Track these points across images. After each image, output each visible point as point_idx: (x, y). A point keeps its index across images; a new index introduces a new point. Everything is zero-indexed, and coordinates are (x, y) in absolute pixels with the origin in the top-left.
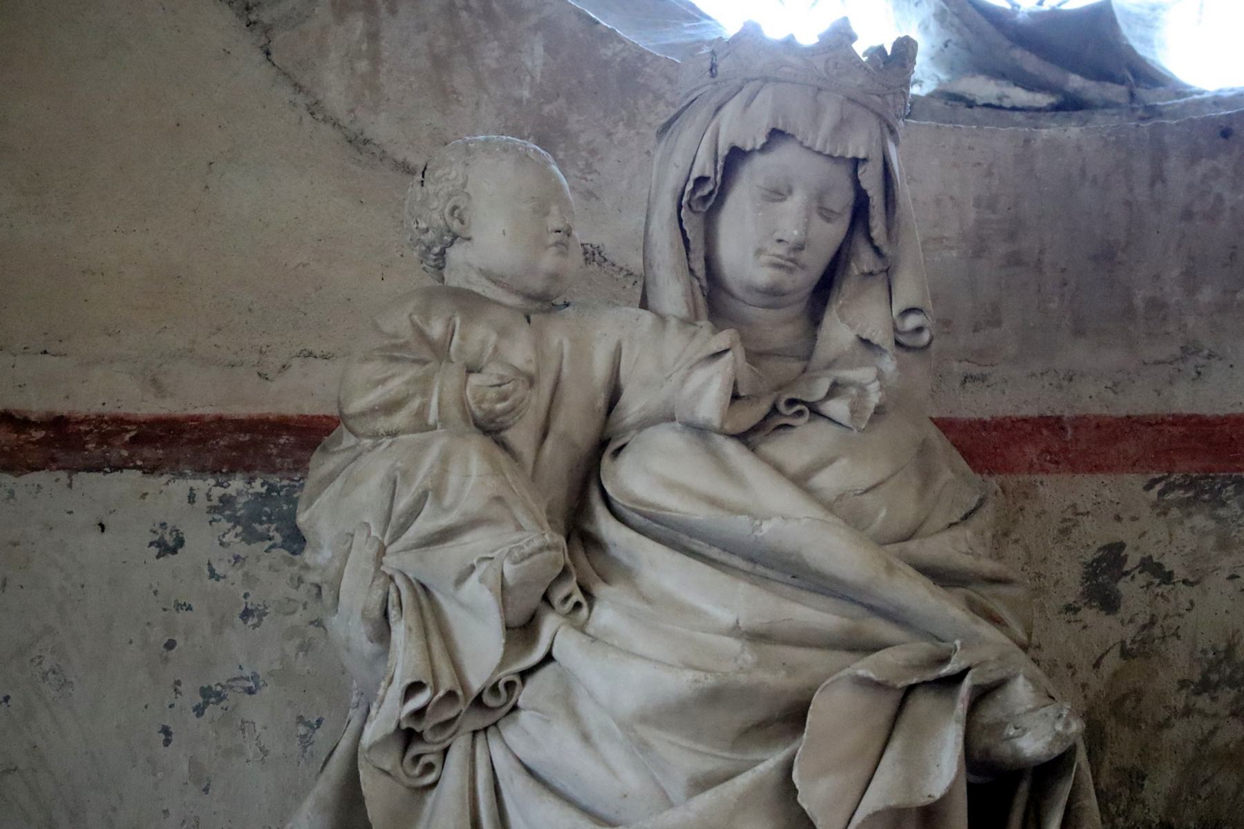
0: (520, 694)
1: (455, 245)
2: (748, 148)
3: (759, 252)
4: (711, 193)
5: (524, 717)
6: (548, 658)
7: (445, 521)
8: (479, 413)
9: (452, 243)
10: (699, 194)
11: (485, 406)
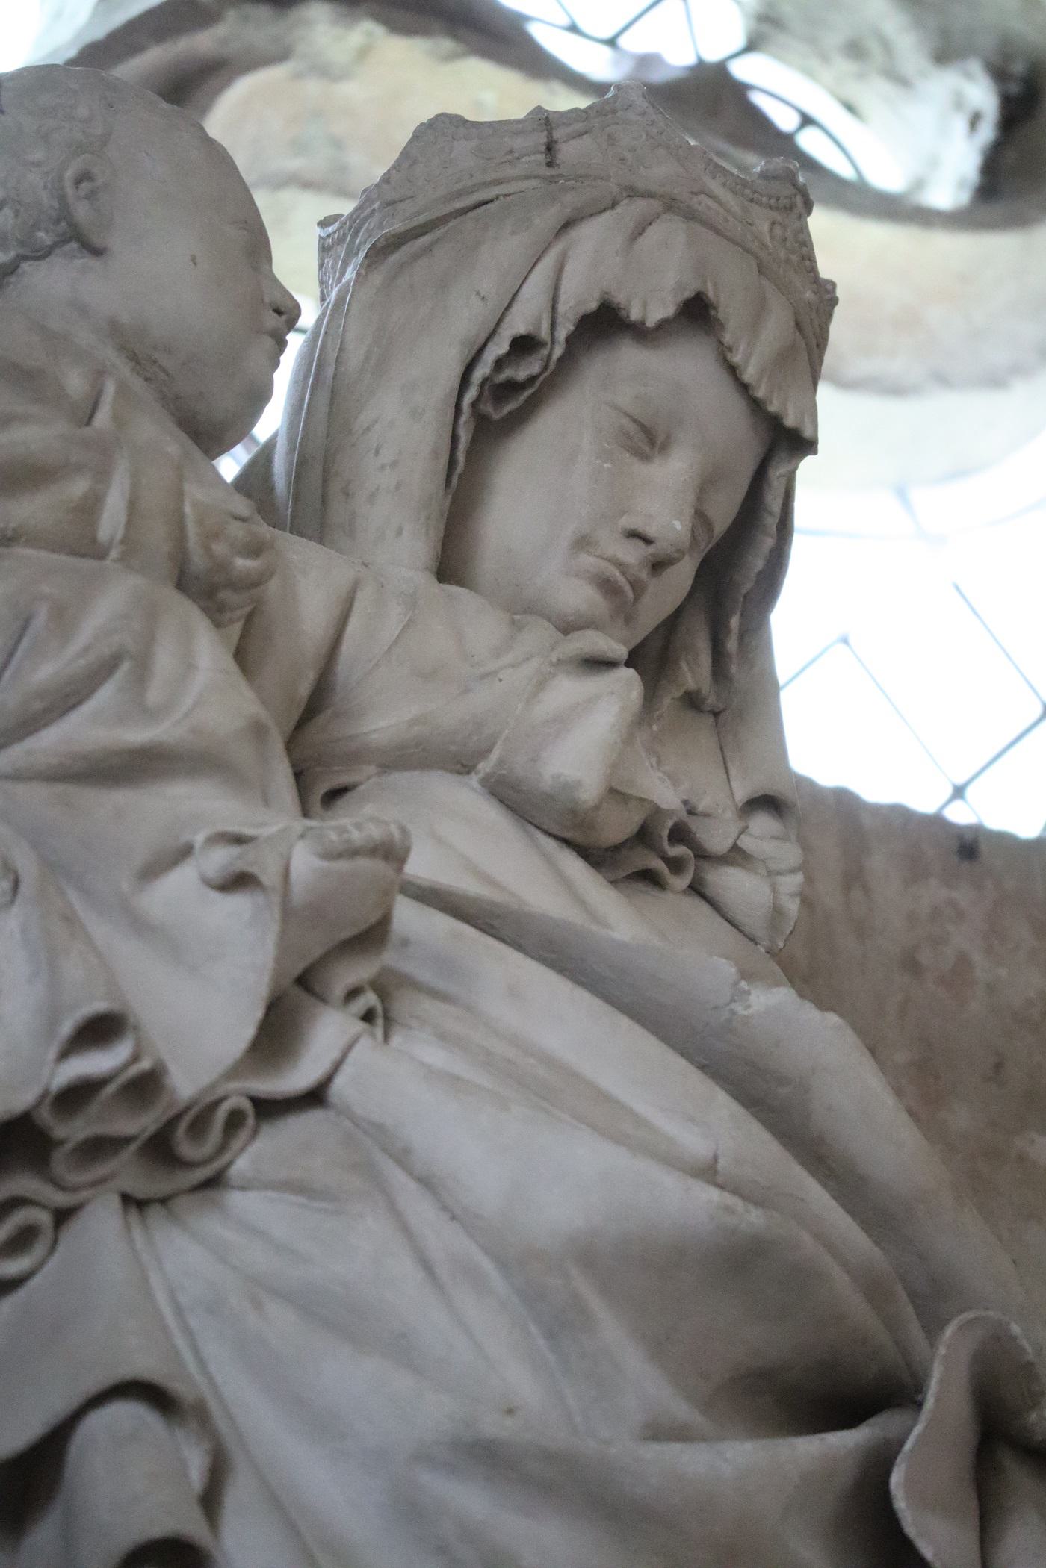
0: (242, 1149)
1: (56, 260)
2: (635, 315)
3: (582, 543)
4: (532, 380)
5: (237, 1200)
6: (315, 1097)
7: (137, 735)
8: (198, 561)
9: (42, 254)
10: (507, 373)
11: (219, 549)
